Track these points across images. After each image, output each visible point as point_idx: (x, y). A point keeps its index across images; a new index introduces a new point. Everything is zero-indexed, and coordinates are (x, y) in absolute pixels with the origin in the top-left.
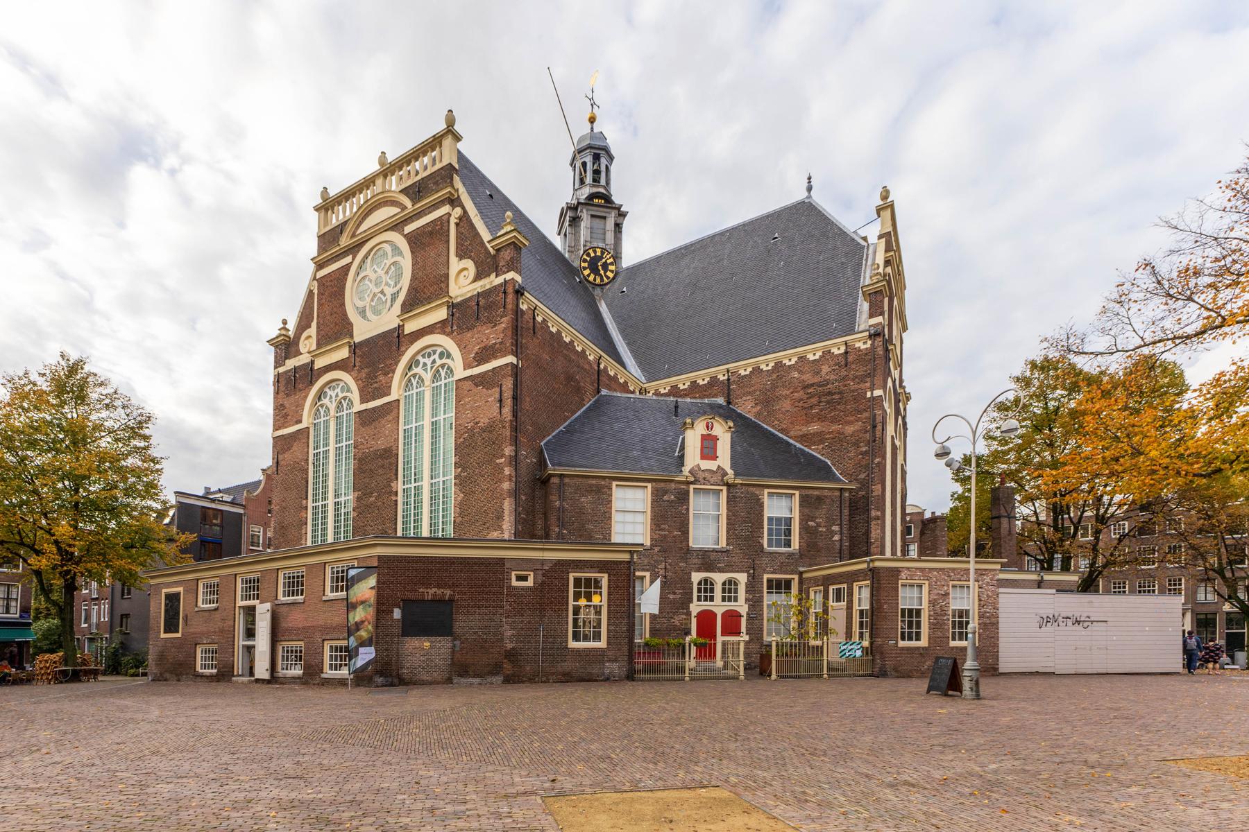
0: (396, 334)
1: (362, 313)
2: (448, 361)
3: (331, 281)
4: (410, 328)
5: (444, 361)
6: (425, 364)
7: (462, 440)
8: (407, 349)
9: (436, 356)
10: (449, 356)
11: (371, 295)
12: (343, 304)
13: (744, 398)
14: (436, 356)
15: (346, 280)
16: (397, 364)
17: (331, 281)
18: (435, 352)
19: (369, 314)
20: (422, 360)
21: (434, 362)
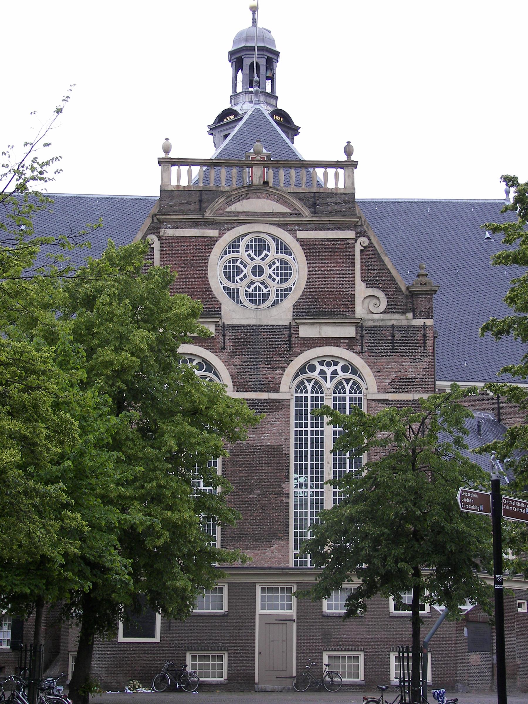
0: (286, 333)
1: (234, 294)
2: (356, 378)
3: (184, 246)
4: (305, 331)
5: (348, 375)
6: (322, 372)
7: (377, 457)
8: (302, 352)
9: (338, 368)
10: (355, 371)
11: (246, 281)
12: (205, 277)
13: (514, 419)
14: (338, 368)
15: (210, 253)
16: (288, 362)
17: (184, 246)
18: (336, 363)
19: (242, 297)
20: (319, 367)
21: (335, 372)
